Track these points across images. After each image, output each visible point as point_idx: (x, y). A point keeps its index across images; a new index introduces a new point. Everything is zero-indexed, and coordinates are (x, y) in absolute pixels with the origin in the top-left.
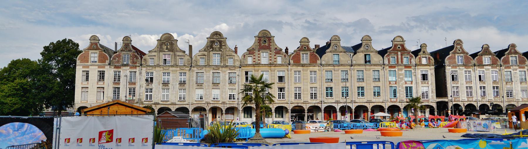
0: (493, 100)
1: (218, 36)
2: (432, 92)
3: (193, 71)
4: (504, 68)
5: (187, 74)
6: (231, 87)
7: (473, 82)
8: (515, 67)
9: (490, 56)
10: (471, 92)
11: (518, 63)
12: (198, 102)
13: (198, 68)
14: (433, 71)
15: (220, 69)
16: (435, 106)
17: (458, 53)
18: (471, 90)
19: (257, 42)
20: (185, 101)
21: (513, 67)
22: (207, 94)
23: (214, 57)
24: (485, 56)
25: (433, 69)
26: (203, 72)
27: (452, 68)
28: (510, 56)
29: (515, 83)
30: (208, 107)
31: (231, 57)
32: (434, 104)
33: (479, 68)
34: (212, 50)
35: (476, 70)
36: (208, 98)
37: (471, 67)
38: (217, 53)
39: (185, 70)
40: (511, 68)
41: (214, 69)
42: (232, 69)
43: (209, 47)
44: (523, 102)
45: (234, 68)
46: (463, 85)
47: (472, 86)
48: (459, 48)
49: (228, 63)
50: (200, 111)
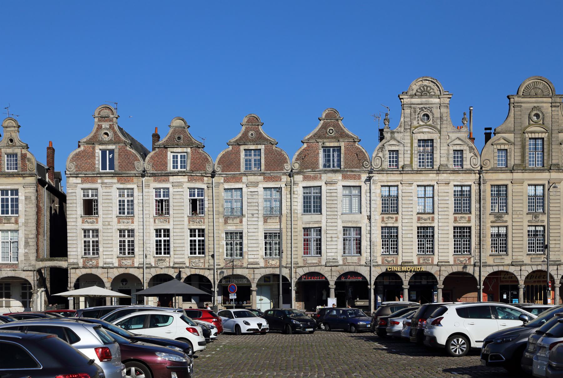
0: (188, 265)
2: (27, 244)
4: (222, 181)
7: (136, 219)
8: (252, 178)
9: (189, 150)
10: (132, 244)
11: (263, 167)
14: (31, 190)
16: (31, 278)
17: (101, 143)
18: (132, 239)
21: (249, 177)
24: (175, 150)
25: (30, 185)
27: (82, 182)
28: (242, 148)
29: (249, 219)
32: (31, 273)
33: (155, 181)
35: (148, 186)
37: (135, 180)
40: (243, 181)
44: (267, 269)
46: (109, 227)
47: (132, 228)
48: (107, 129)
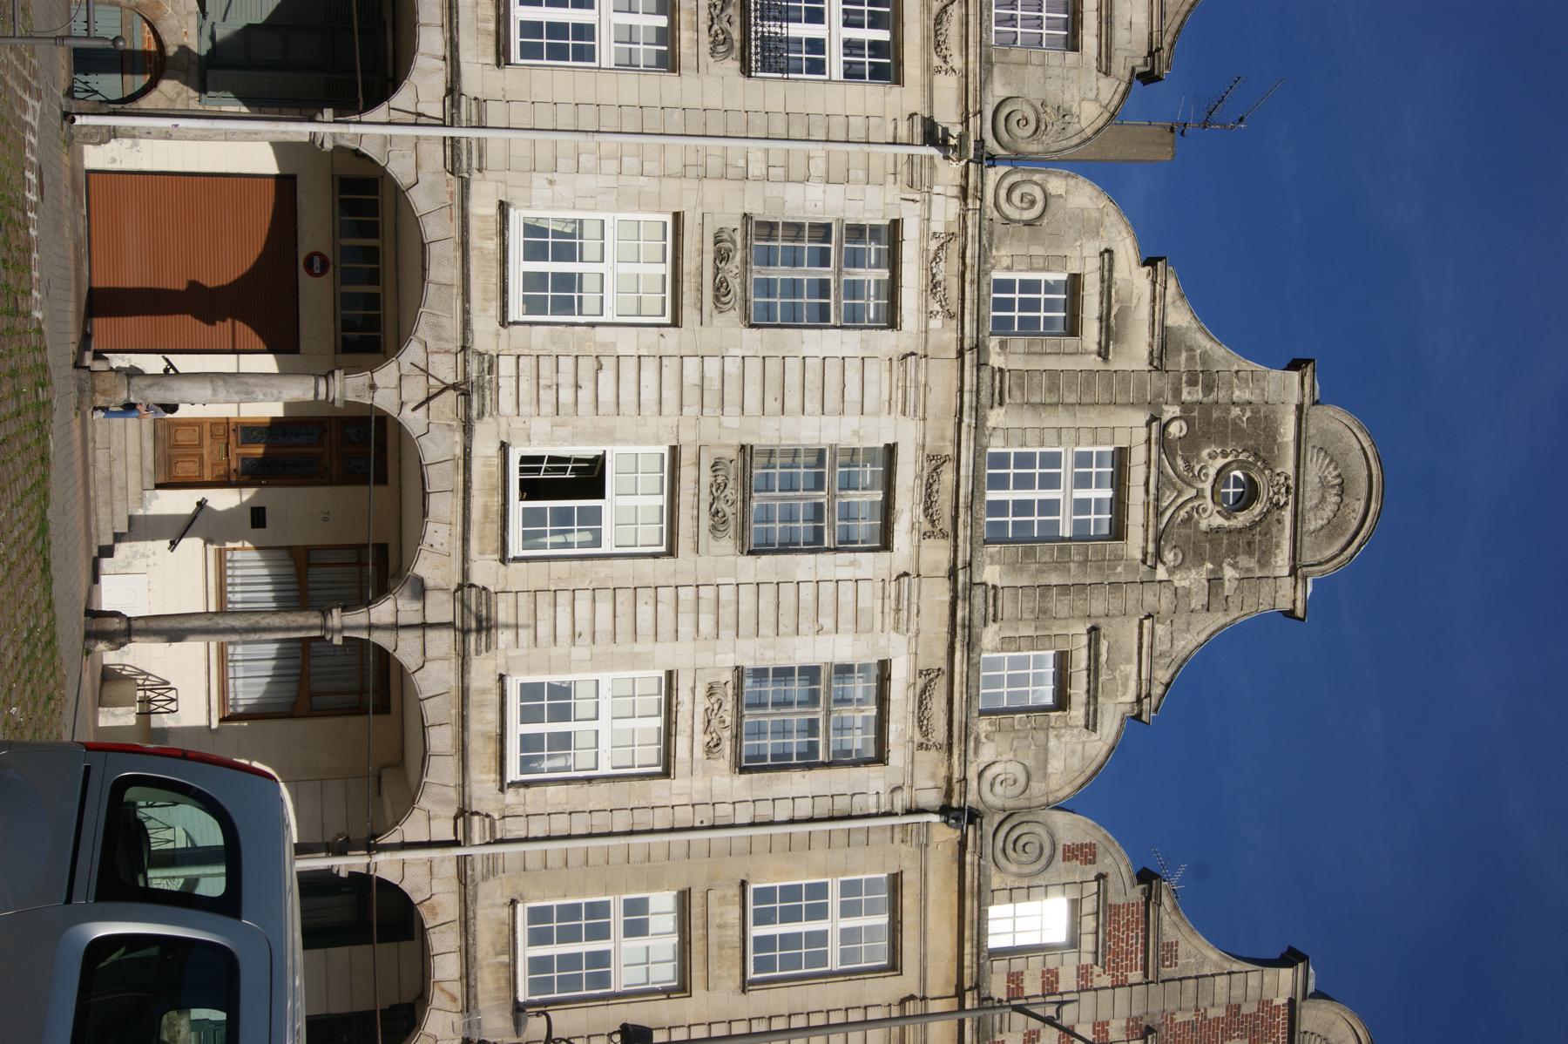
1: (1328, 512)
3: (917, 182)
5: (870, 97)
6: (691, 707)
12: (493, 245)
13: (955, 247)
15: (937, 554)
19: (1237, 993)
20: (502, 56)
22: (607, 377)
23: (1083, 459)
26: (891, 320)
30: (415, 390)
31: (1078, 690)
34: (1175, 430)
36: (547, 396)
38: (1136, 496)
39: (930, 71)
41: (934, 463)
42: (937, 704)
43: (1208, 389)
45: (939, 734)
49: (1007, 643)
50: (348, 253)
